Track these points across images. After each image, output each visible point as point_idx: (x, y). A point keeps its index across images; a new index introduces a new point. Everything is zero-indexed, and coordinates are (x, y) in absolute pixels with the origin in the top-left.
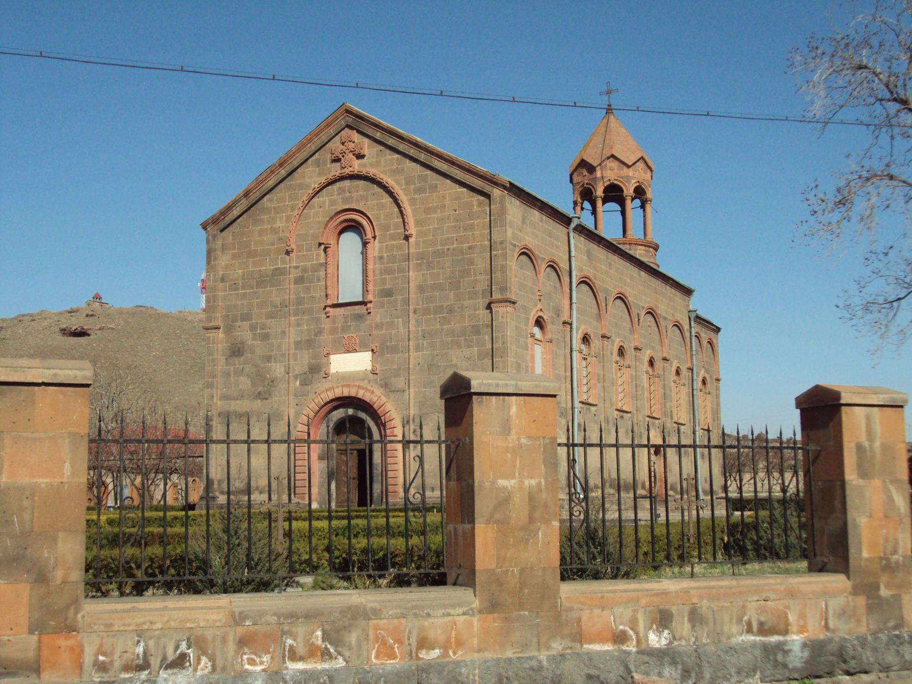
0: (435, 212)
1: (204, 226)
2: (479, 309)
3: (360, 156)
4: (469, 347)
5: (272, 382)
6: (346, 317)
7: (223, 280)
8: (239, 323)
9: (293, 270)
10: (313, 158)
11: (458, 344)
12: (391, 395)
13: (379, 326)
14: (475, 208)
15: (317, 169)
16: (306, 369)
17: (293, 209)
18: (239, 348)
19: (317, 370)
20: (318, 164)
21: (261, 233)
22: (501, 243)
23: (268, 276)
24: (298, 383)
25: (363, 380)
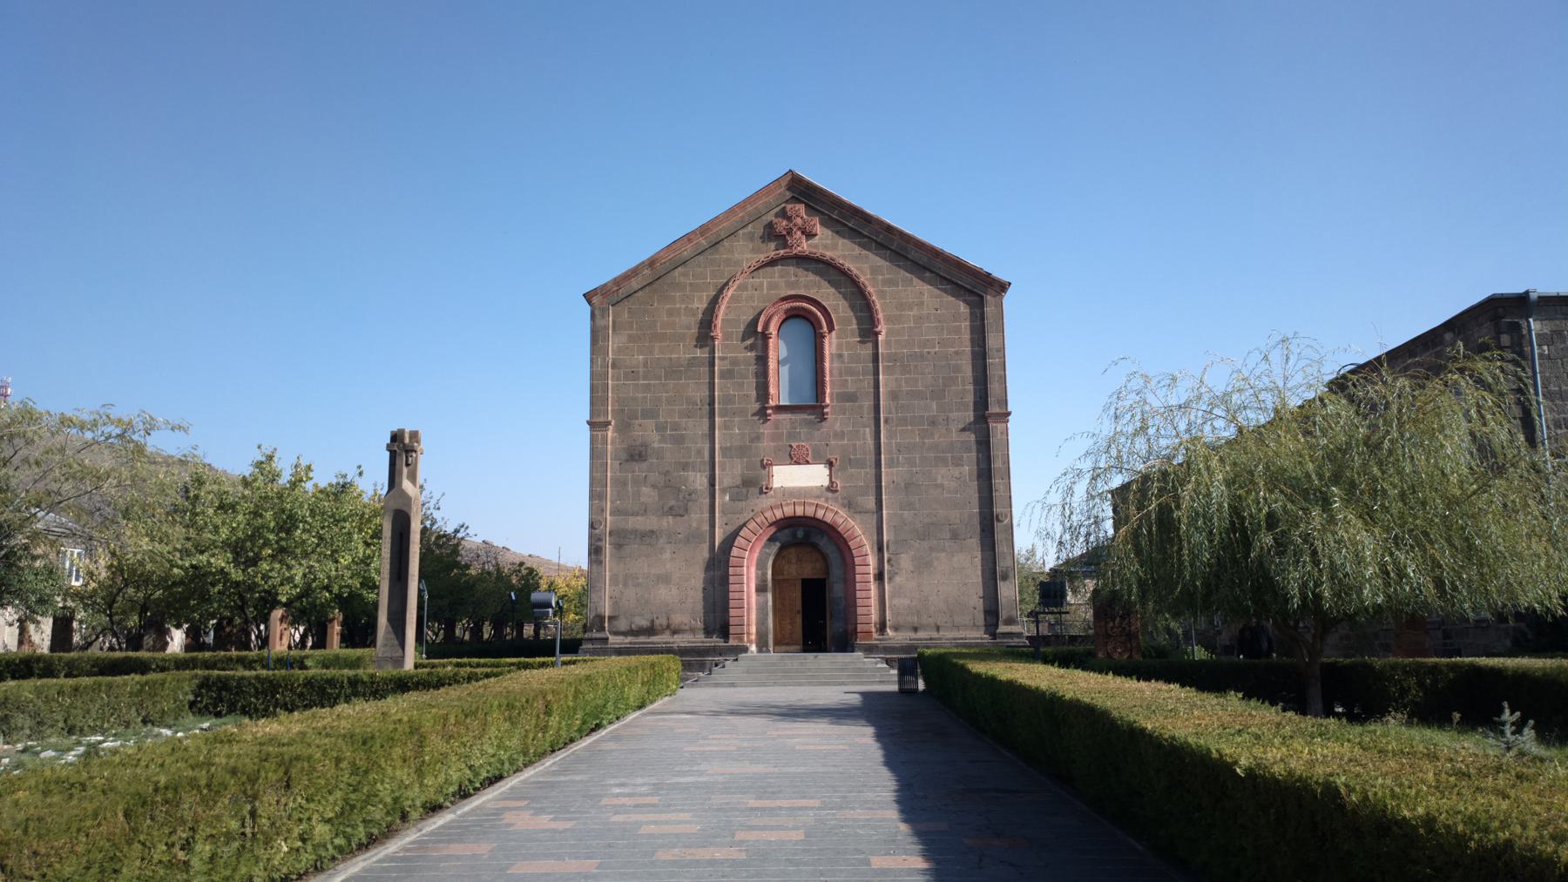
0: (911, 309)
1: (588, 297)
4: (957, 465)
5: (690, 495)
8: (640, 421)
10: (745, 230)
11: (944, 462)
12: (857, 516)
13: (840, 435)
15: (751, 246)
16: (738, 481)
18: (641, 452)
19: (754, 483)
20: (751, 237)
21: (670, 313)
22: (998, 350)
23: (682, 366)
24: (727, 498)
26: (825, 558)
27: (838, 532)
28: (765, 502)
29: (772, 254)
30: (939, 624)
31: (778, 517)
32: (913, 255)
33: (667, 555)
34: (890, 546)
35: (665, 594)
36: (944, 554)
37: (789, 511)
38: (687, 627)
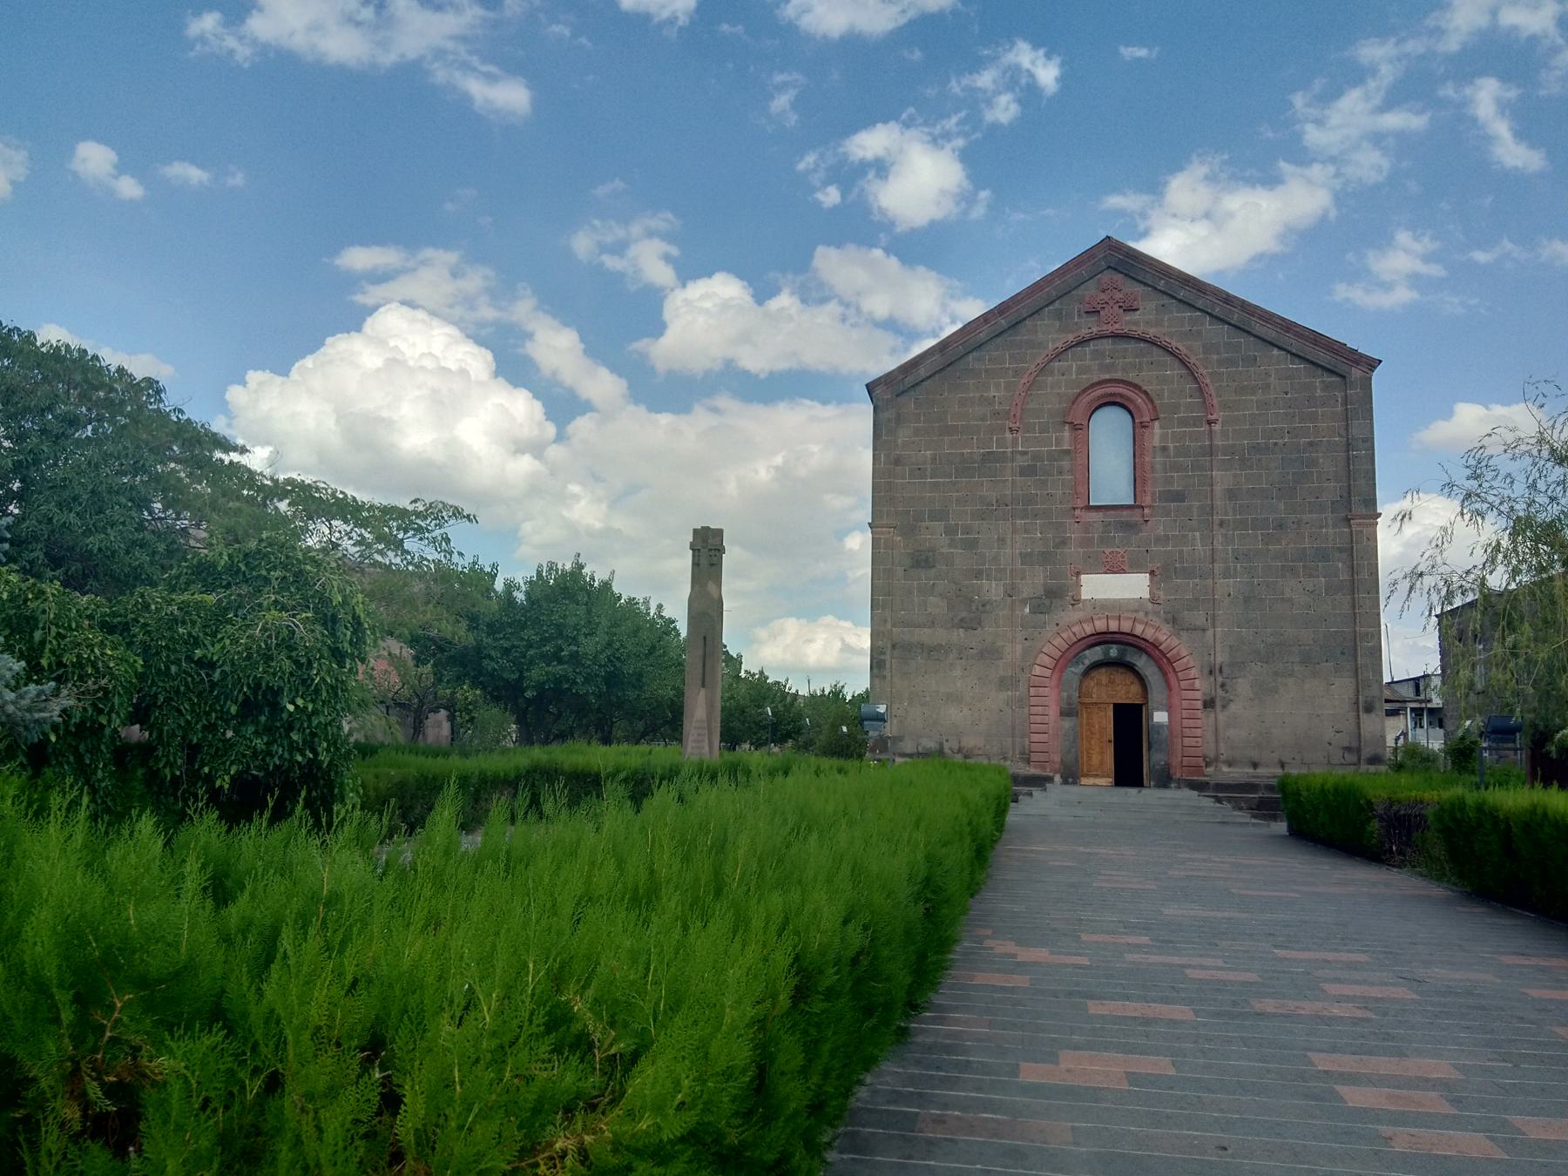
2: (1327, 526)
3: (1132, 310)
4: (1311, 576)
6: (1106, 525)
7: (897, 462)
9: (1018, 457)
10: (1051, 308)
12: (1184, 634)
14: (1319, 393)
15: (1057, 323)
17: (1017, 373)
18: (927, 557)
19: (1058, 594)
20: (1058, 315)
22: (1365, 440)
24: (1027, 610)
25: (1136, 611)
26: (1141, 680)
27: (1160, 651)
28: (1071, 615)
29: (1084, 332)
30: (1284, 760)
31: (1089, 633)
32: (1259, 328)
33: (957, 672)
34: (1225, 670)
35: (954, 715)
36: (1291, 681)
37: (1100, 625)
38: (980, 753)
